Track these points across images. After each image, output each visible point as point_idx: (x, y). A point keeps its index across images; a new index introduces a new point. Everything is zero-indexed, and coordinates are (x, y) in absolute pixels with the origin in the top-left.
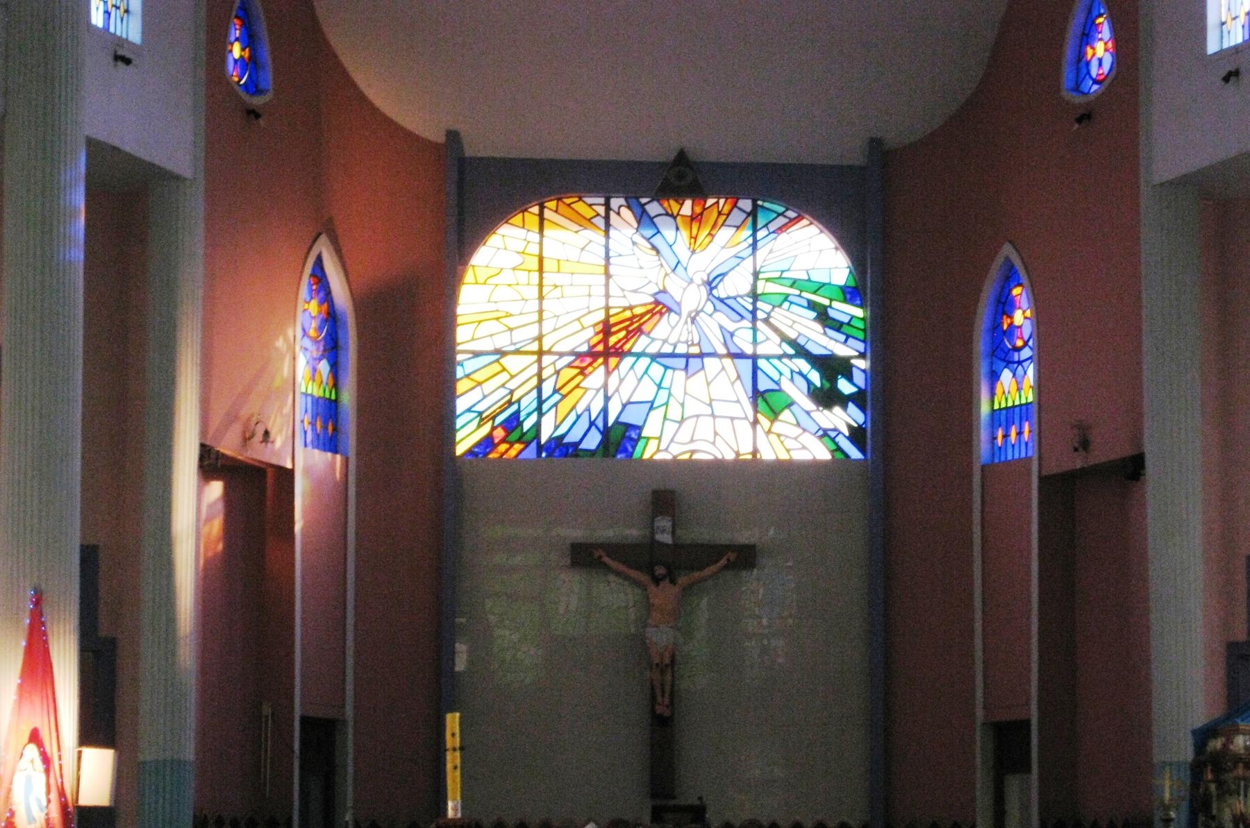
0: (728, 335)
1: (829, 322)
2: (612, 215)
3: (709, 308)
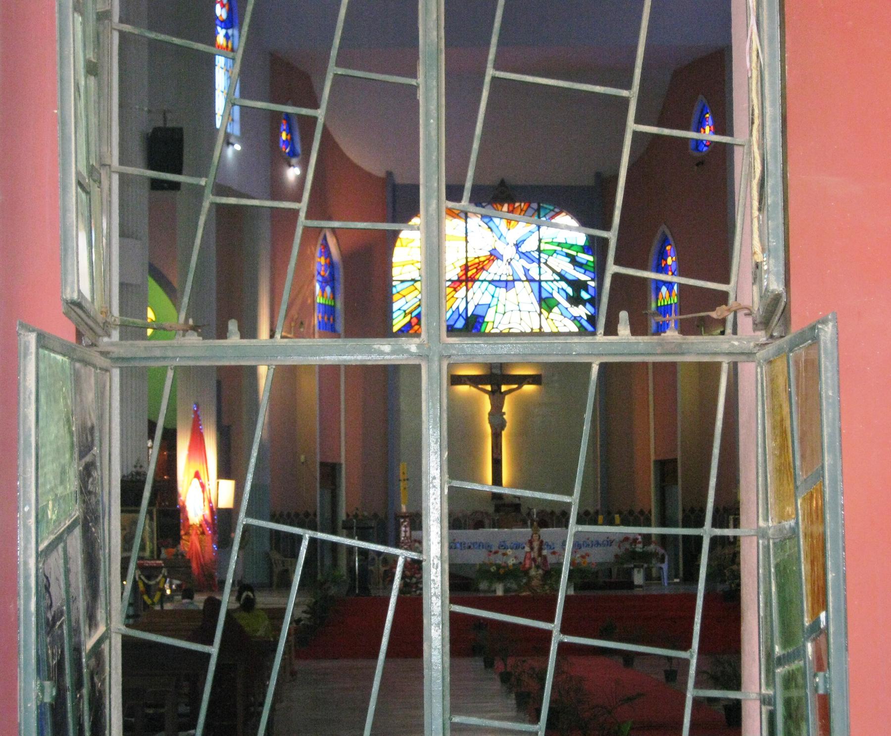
0: (527, 271)
3: (517, 257)
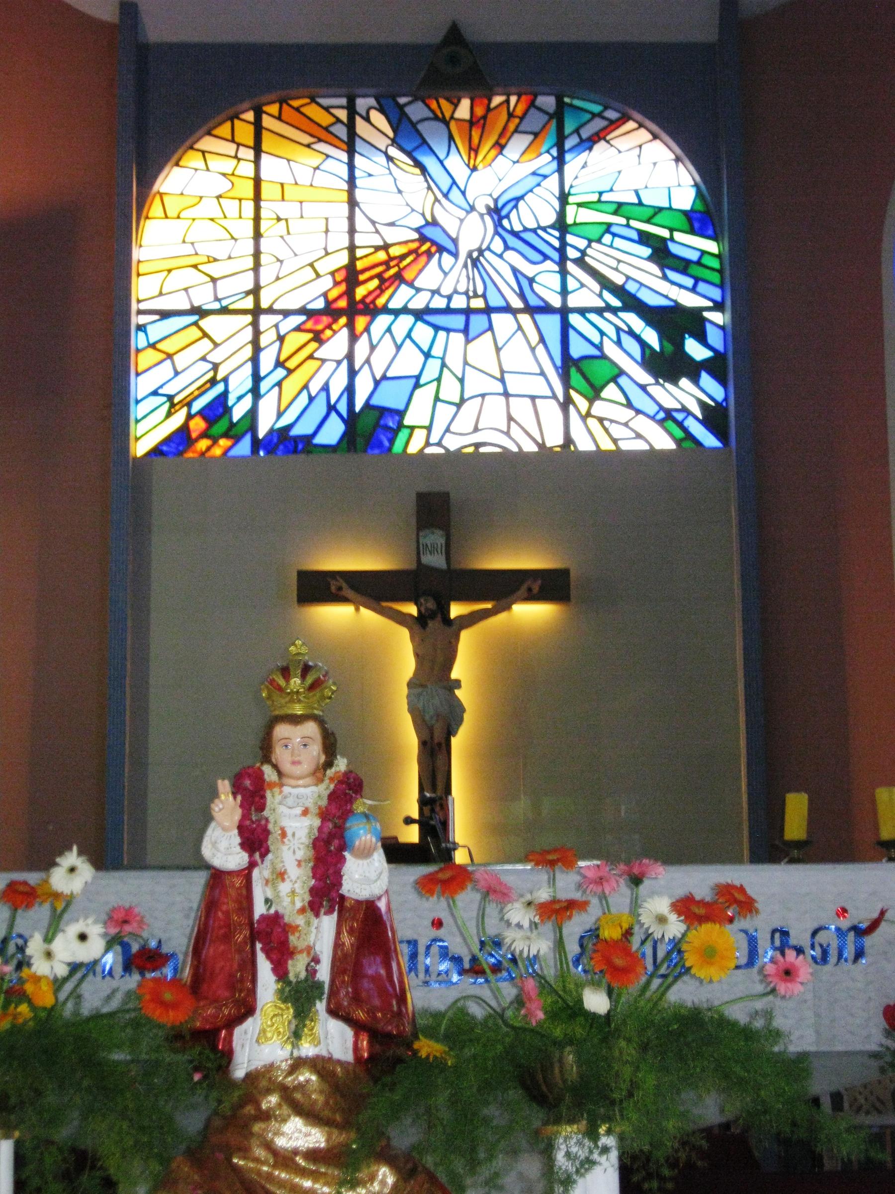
1: (670, 261)
2: (358, 120)
3: (498, 245)
